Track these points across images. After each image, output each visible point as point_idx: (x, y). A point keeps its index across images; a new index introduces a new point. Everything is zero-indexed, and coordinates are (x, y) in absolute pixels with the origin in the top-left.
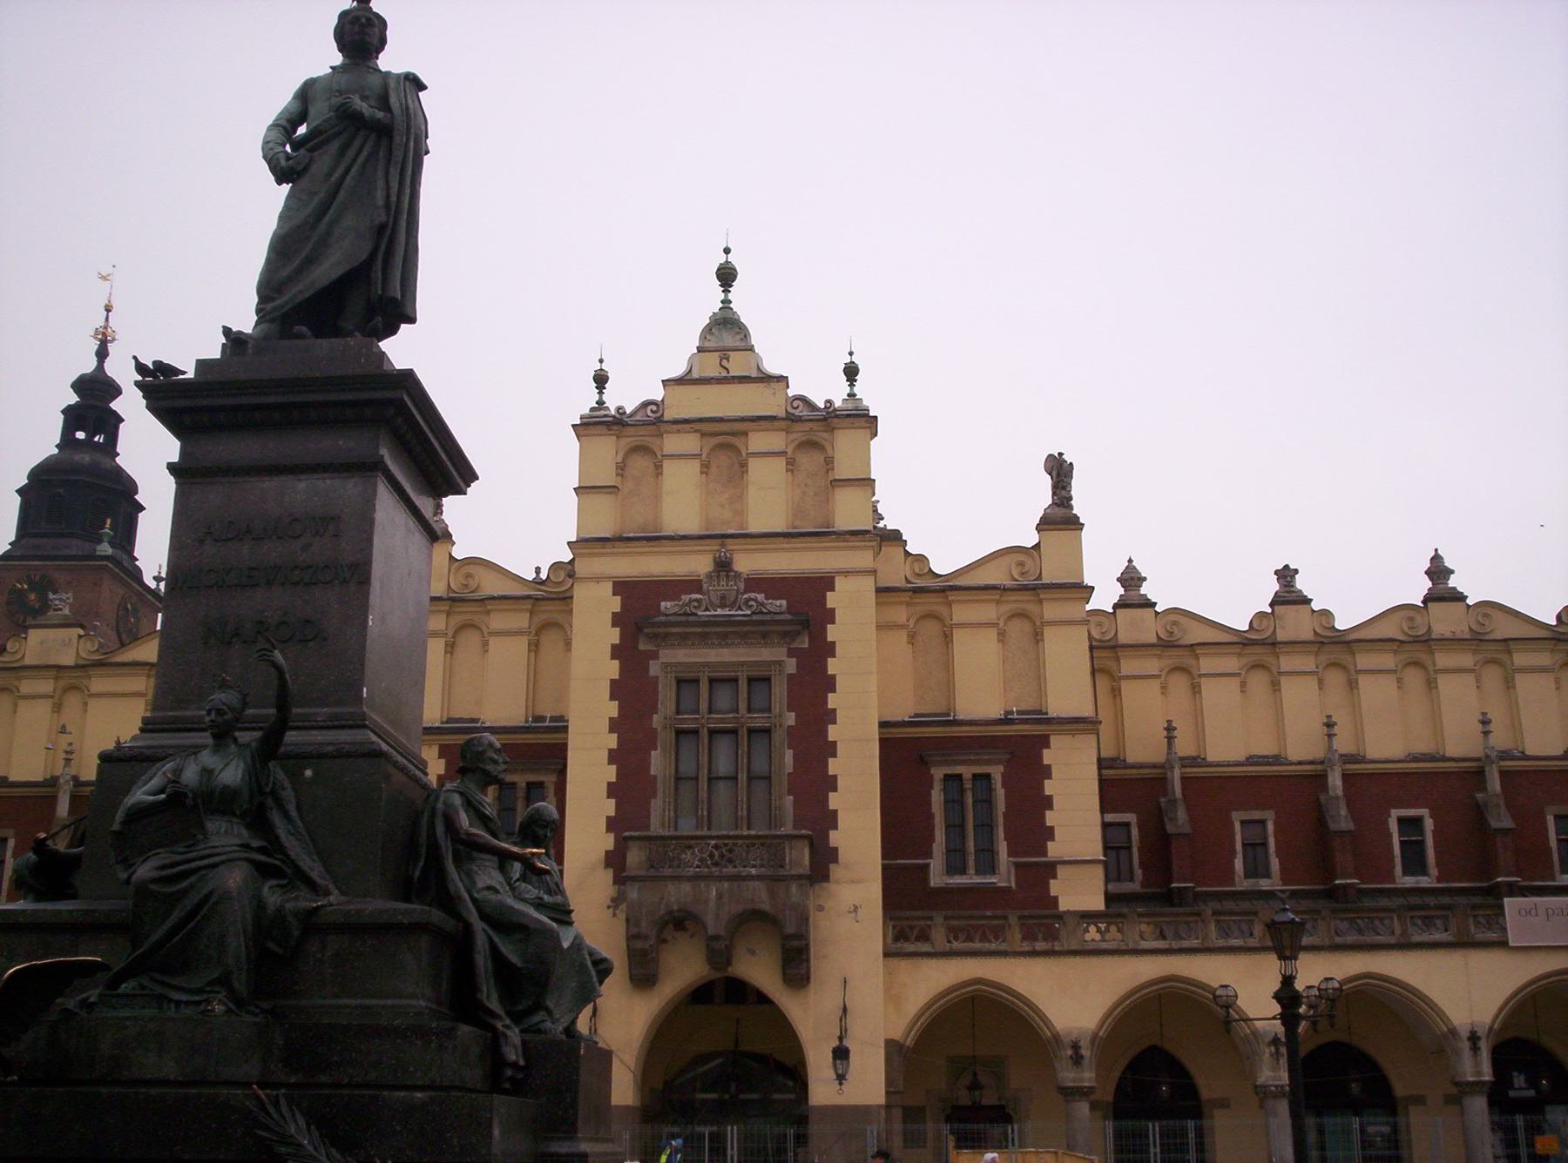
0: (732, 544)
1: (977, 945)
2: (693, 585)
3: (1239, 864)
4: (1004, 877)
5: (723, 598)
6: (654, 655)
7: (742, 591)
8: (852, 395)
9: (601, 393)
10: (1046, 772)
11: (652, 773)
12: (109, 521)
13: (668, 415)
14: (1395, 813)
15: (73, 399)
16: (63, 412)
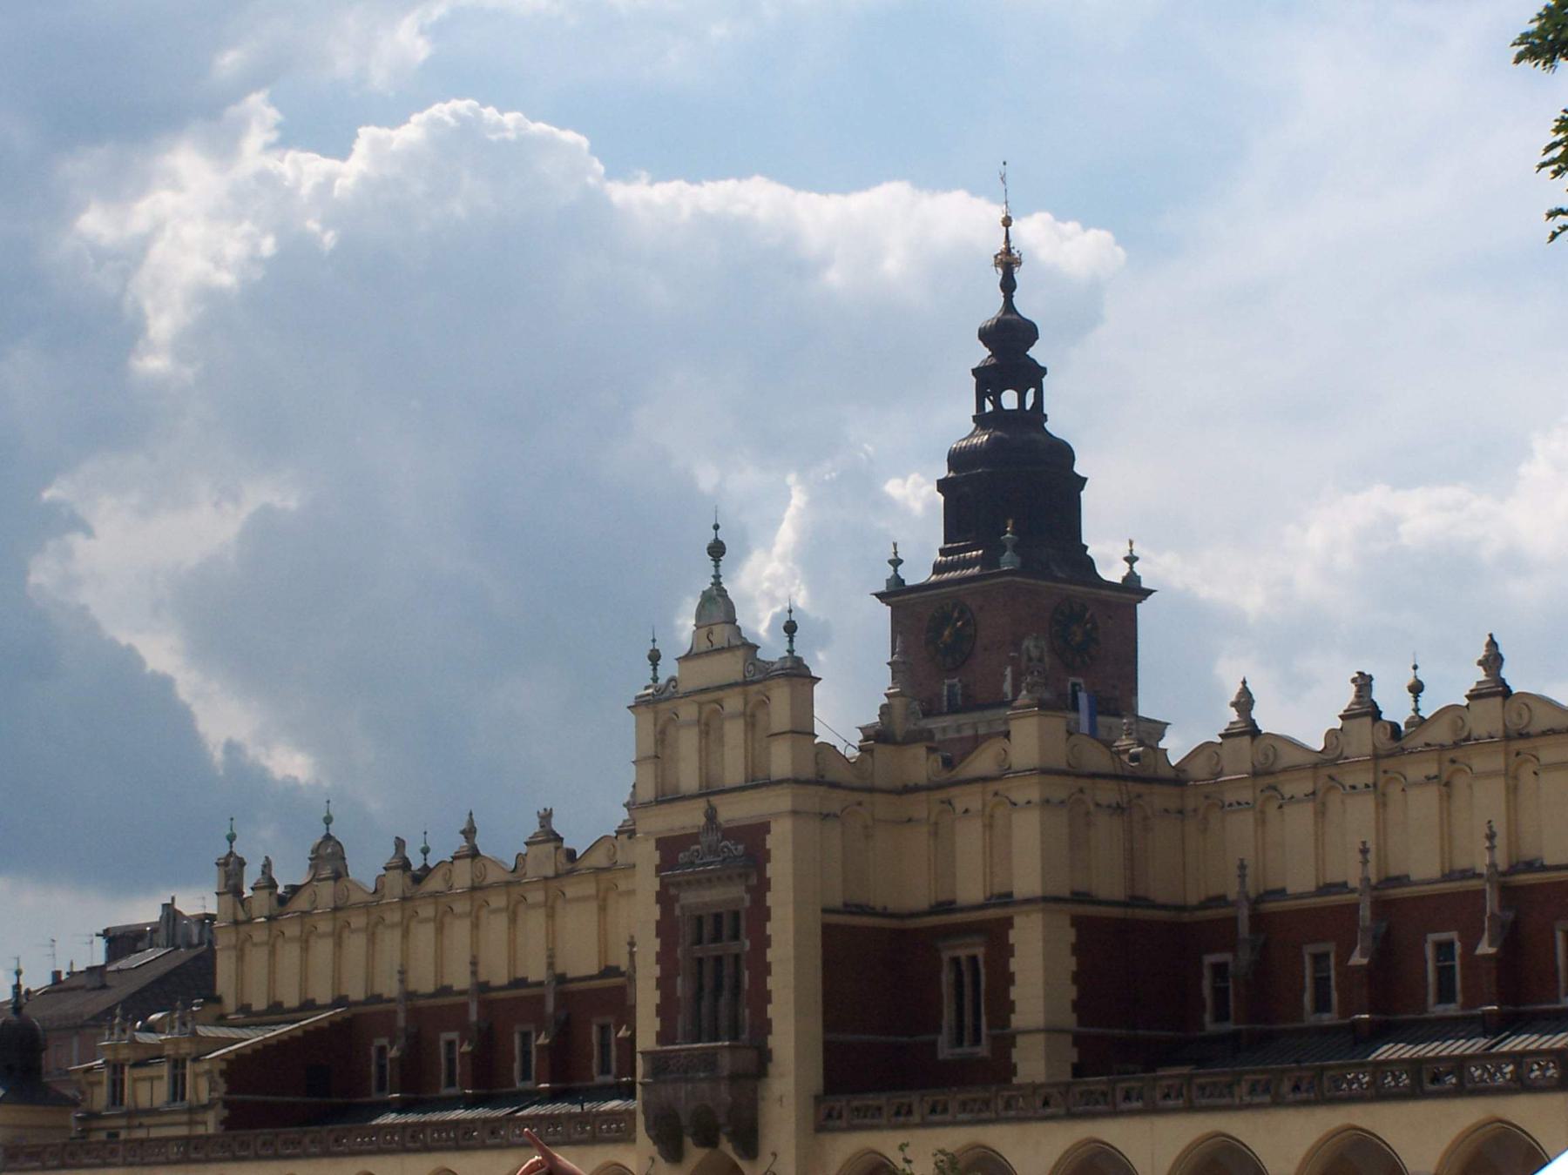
0: (715, 800)
1: (867, 1121)
2: (692, 838)
3: (1308, 998)
4: (983, 1050)
5: (710, 846)
6: (676, 899)
7: (720, 838)
8: (791, 651)
9: (655, 669)
10: (1008, 951)
11: (679, 993)
12: (1010, 522)
13: (682, 689)
14: (1432, 937)
15: (981, 354)
16: (975, 372)
